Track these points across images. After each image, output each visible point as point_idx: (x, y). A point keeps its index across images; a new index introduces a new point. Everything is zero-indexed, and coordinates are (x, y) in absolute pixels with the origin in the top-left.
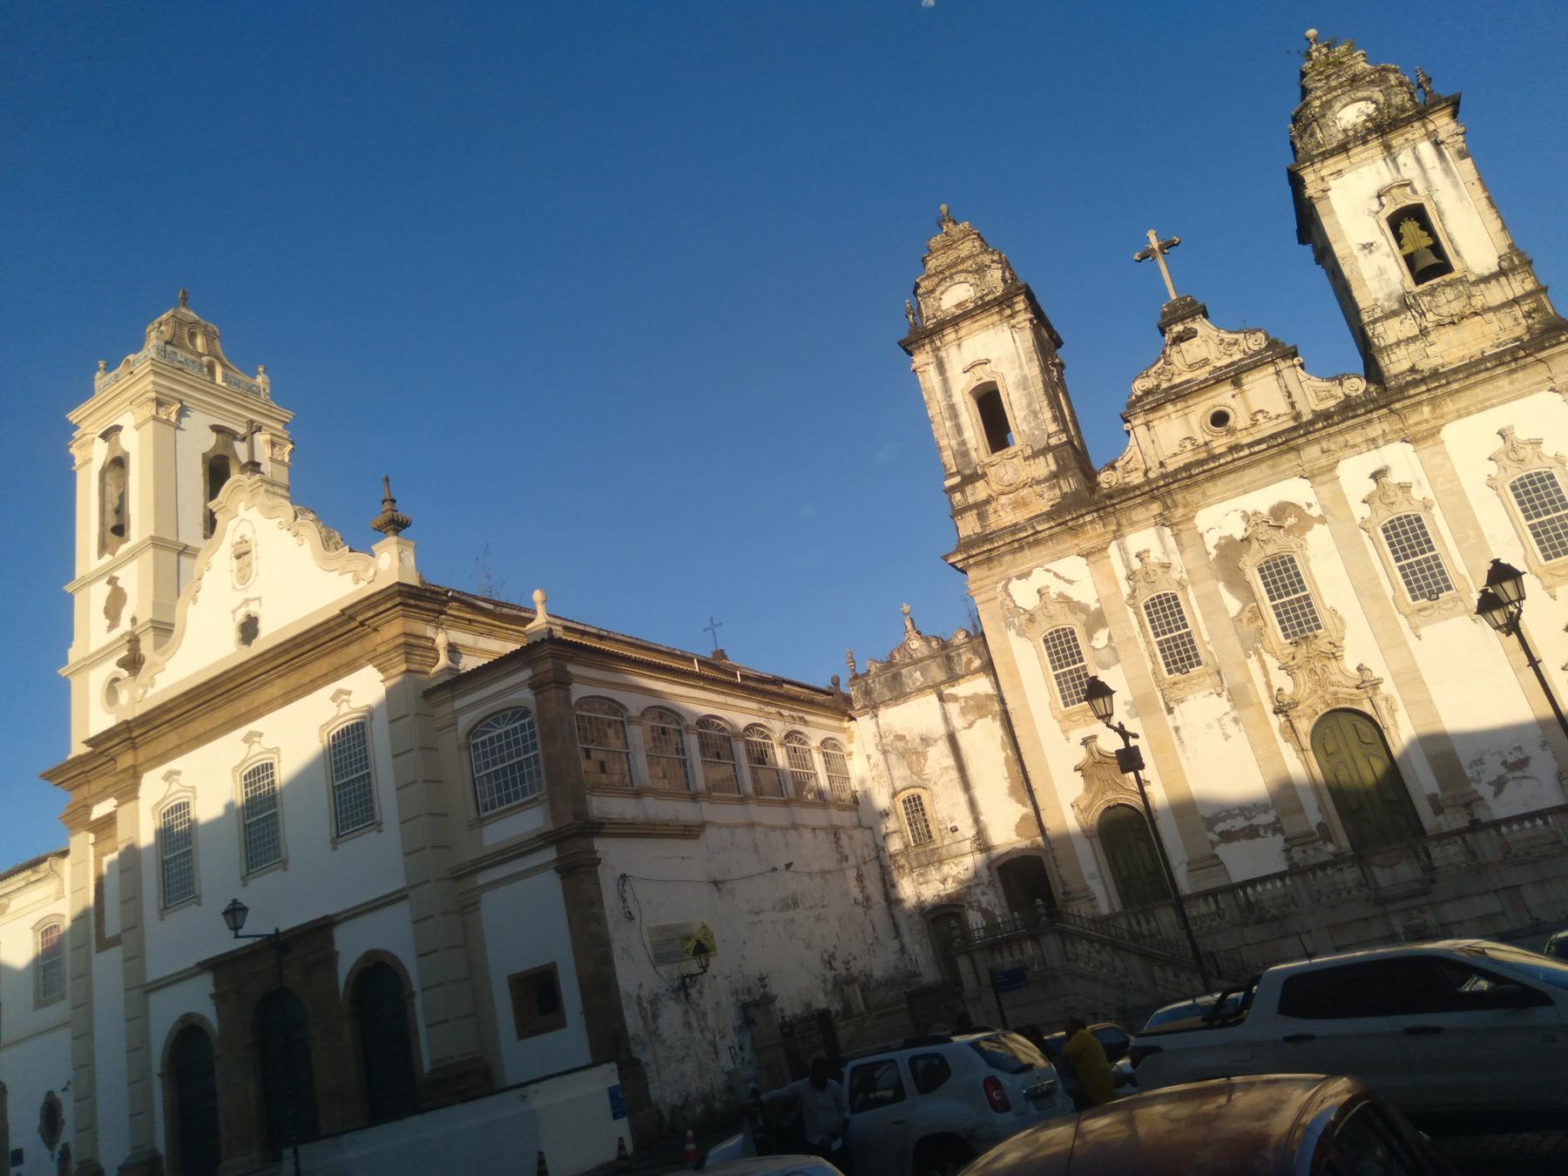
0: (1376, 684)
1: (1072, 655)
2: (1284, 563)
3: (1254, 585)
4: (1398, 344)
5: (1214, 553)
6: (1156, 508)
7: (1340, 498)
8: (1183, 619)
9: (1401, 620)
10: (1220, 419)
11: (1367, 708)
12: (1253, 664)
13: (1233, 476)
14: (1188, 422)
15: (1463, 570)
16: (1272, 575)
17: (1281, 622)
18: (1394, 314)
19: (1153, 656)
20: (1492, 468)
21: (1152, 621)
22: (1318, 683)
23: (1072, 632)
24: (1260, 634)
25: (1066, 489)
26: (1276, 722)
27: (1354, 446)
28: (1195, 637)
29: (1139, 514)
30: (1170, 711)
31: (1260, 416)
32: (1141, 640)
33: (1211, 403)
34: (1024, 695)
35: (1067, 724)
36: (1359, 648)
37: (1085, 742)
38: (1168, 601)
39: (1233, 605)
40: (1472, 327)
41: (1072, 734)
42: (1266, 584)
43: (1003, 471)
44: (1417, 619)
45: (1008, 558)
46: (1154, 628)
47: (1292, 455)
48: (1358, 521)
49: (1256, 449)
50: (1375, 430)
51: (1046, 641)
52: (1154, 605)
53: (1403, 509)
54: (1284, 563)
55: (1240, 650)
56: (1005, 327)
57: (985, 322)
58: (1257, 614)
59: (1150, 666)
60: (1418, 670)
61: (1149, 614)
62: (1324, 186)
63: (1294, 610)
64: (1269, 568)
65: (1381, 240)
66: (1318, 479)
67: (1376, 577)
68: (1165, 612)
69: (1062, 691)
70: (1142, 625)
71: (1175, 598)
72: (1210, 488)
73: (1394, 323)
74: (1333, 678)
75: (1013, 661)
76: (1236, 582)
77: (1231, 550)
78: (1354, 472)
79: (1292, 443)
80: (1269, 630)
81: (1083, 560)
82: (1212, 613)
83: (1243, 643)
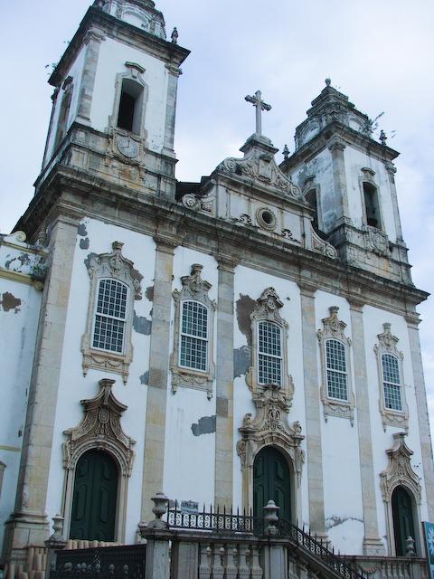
1: (117, 308)
3: (254, 333)
4: (357, 247)
5: (237, 298)
6: (214, 244)
7: (312, 309)
8: (205, 329)
9: (321, 403)
10: (267, 217)
11: (291, 452)
13: (262, 257)
14: (249, 206)
15: (354, 392)
18: (359, 231)
19: (176, 344)
20: (377, 341)
21: (184, 318)
23: (125, 291)
25: (162, 188)
26: (237, 438)
27: (326, 285)
28: (208, 347)
29: (203, 240)
30: (174, 392)
31: (286, 233)
32: (172, 327)
33: (265, 206)
34: (65, 318)
35: (88, 361)
36: (297, 413)
37: (106, 383)
38: (200, 310)
39: (240, 340)
40: (383, 263)
41: (90, 372)
42: (261, 338)
43: (126, 144)
44: (328, 410)
45: (99, 206)
46: (184, 324)
48: (317, 331)
49: (286, 250)
50: (338, 284)
51: (102, 285)
52: (190, 308)
53: (339, 339)
56: (163, 63)
57: (149, 49)
59: (171, 351)
60: (320, 441)
61: (184, 312)
62: (344, 143)
63: (270, 365)
64: (265, 328)
65: (358, 188)
66: (306, 292)
67: (317, 370)
68: (195, 317)
69: (96, 331)
70: (176, 318)
71: (205, 312)
73: (357, 235)
74: (281, 423)
75: (69, 283)
76: (245, 325)
77: (246, 305)
78: (325, 300)
81: (154, 246)
82: (226, 337)
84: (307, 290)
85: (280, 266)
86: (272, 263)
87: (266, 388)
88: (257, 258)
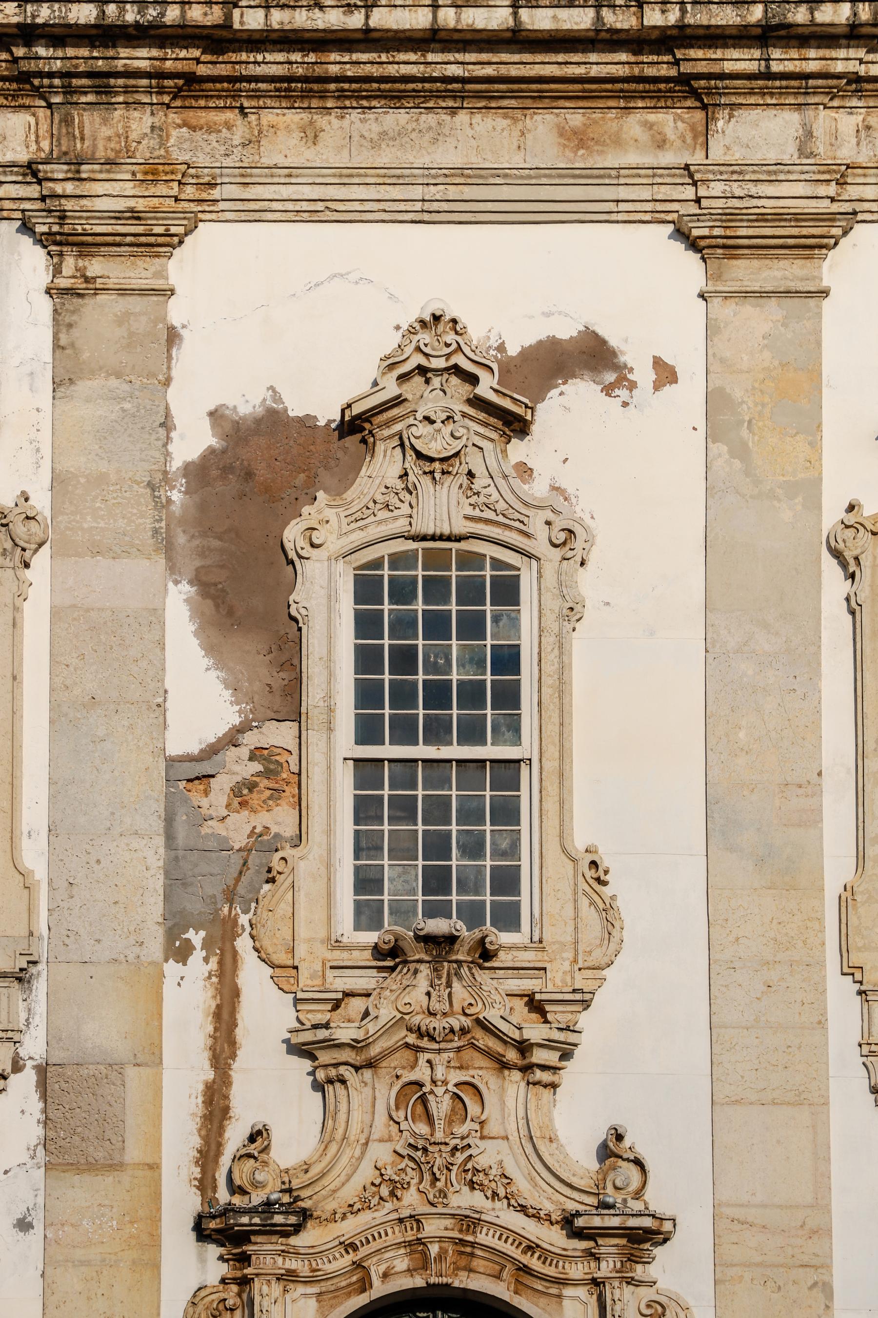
0: (643, 1239)
2: (471, 592)
12: (187, 990)
13: (396, 119)
16: (403, 625)
17: (365, 846)
22: (418, 1153)
24: (262, 865)
47: (673, 122)
54: (471, 592)
55: (155, 907)
58: (277, 778)
60: (823, 1232)
72: (285, 134)
79: (699, 59)
80: (305, 864)
83: (175, 880)
84: (761, 249)
85: (536, 138)
86: (477, 137)
87: (390, 956)
88: (348, 136)
